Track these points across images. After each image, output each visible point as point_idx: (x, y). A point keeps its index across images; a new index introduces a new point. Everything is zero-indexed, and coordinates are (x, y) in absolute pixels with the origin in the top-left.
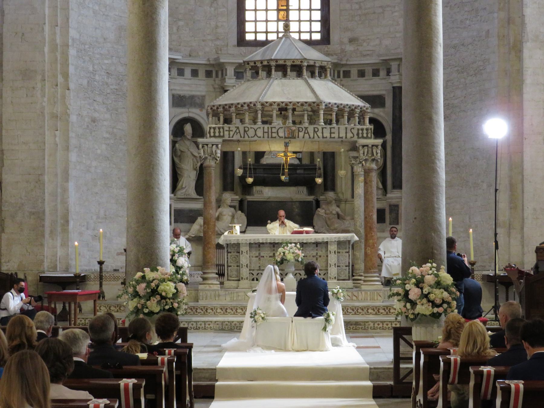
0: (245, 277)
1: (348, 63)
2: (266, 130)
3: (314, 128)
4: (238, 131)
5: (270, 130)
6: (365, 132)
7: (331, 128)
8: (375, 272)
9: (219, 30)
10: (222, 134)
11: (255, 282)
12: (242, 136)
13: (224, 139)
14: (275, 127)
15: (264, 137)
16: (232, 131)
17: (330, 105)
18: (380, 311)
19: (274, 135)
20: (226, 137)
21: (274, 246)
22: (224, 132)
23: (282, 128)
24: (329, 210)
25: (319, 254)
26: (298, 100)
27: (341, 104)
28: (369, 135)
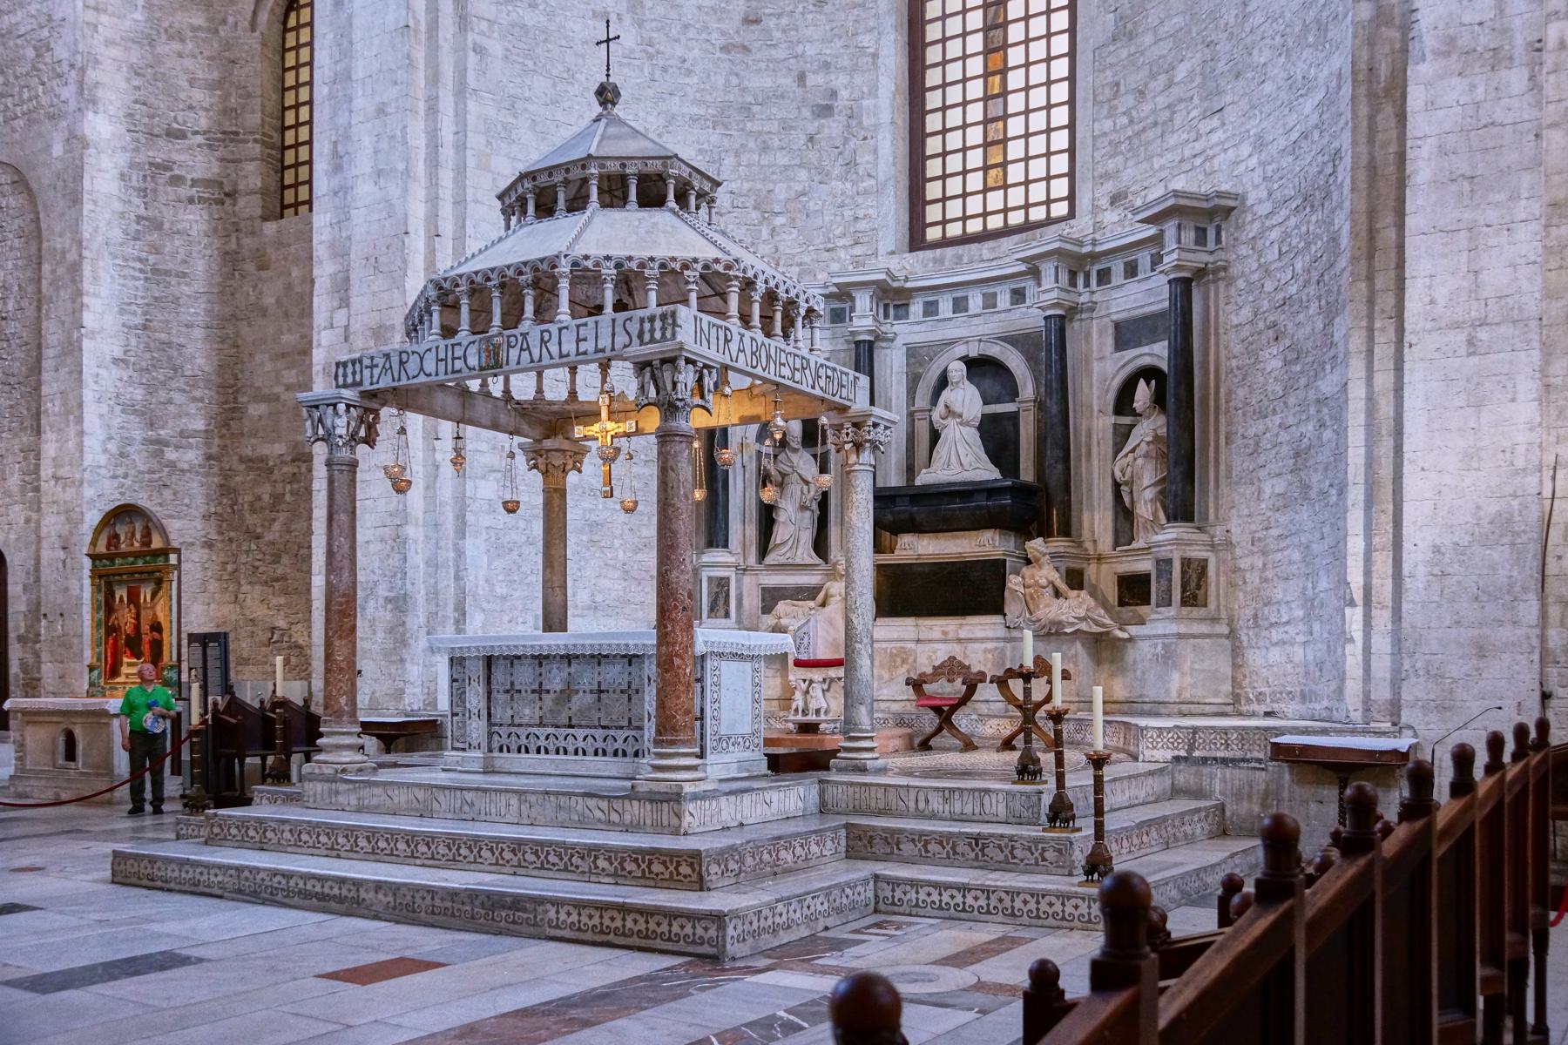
0: (475, 743)
1: (1098, 249)
2: (442, 356)
3: (542, 332)
4: (387, 366)
5: (450, 353)
6: (658, 324)
7: (578, 327)
8: (684, 743)
9: (862, 226)
10: (358, 378)
11: (505, 754)
12: (396, 377)
13: (362, 389)
14: (460, 344)
15: (437, 374)
16: (377, 366)
17: (589, 264)
18: (626, 864)
19: (459, 364)
20: (367, 386)
21: (540, 665)
22: (361, 372)
23: (474, 342)
24: (1032, 577)
25: (633, 686)
26: (508, 262)
27: (630, 258)
28: (668, 335)
